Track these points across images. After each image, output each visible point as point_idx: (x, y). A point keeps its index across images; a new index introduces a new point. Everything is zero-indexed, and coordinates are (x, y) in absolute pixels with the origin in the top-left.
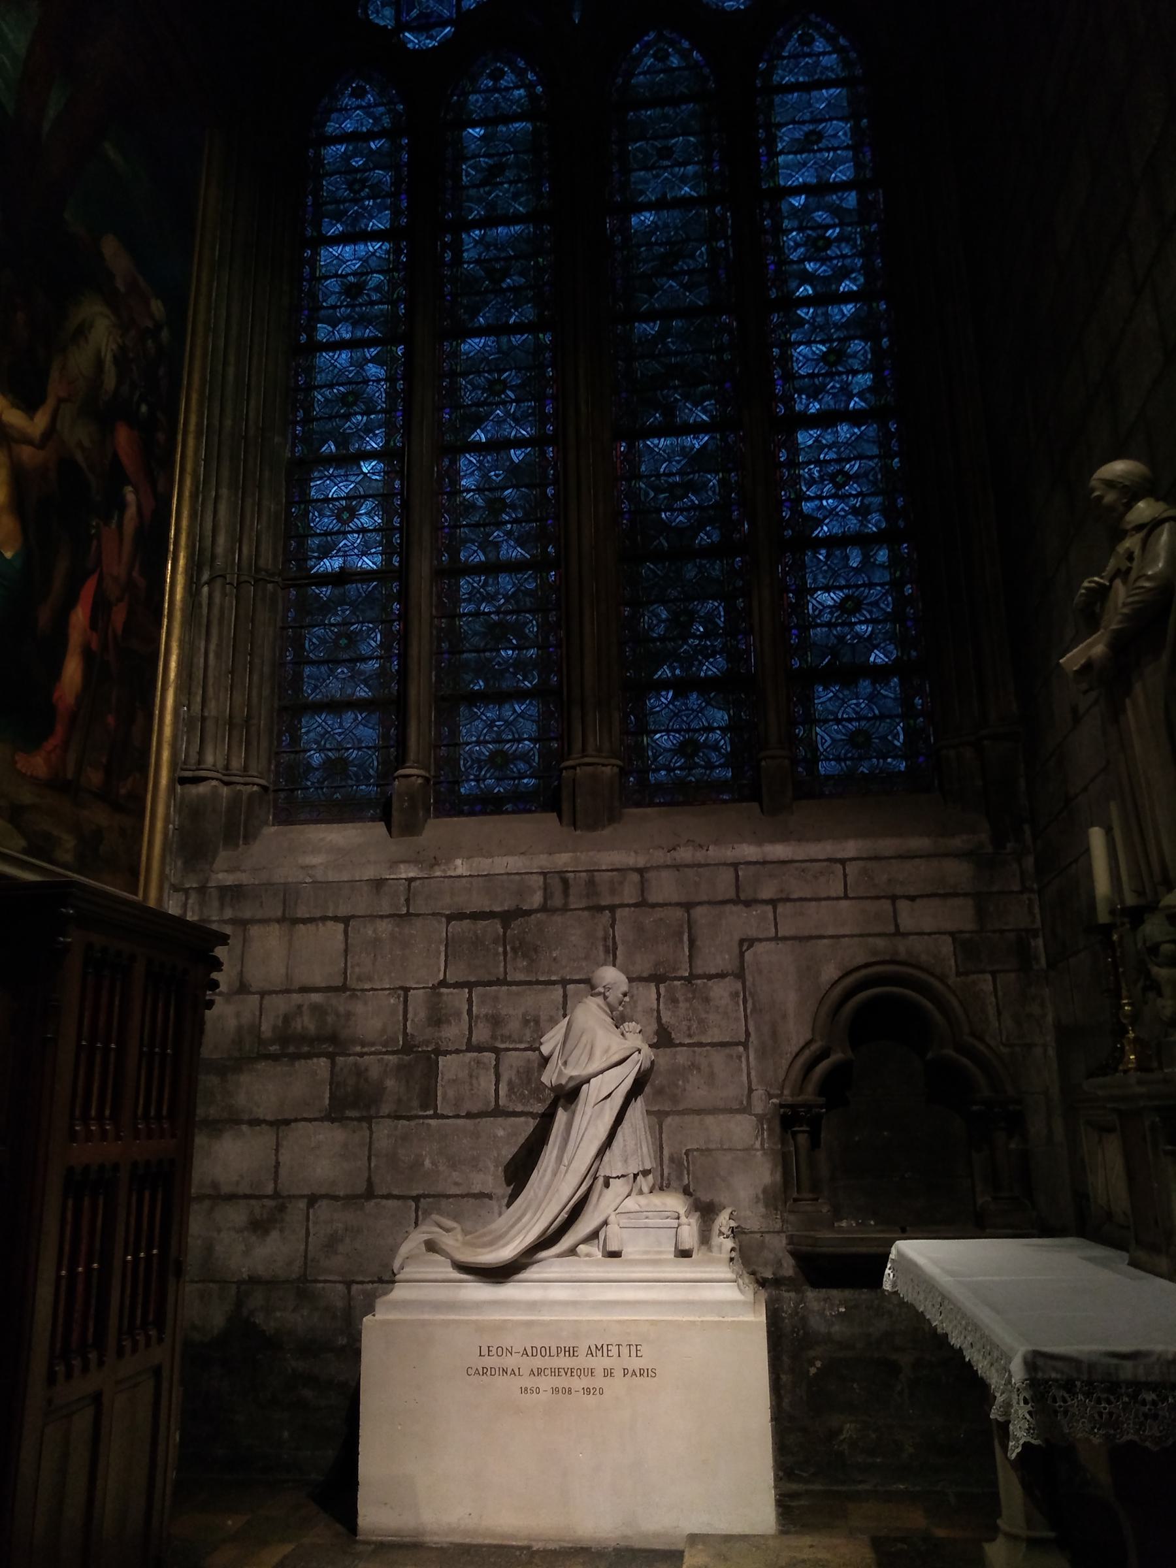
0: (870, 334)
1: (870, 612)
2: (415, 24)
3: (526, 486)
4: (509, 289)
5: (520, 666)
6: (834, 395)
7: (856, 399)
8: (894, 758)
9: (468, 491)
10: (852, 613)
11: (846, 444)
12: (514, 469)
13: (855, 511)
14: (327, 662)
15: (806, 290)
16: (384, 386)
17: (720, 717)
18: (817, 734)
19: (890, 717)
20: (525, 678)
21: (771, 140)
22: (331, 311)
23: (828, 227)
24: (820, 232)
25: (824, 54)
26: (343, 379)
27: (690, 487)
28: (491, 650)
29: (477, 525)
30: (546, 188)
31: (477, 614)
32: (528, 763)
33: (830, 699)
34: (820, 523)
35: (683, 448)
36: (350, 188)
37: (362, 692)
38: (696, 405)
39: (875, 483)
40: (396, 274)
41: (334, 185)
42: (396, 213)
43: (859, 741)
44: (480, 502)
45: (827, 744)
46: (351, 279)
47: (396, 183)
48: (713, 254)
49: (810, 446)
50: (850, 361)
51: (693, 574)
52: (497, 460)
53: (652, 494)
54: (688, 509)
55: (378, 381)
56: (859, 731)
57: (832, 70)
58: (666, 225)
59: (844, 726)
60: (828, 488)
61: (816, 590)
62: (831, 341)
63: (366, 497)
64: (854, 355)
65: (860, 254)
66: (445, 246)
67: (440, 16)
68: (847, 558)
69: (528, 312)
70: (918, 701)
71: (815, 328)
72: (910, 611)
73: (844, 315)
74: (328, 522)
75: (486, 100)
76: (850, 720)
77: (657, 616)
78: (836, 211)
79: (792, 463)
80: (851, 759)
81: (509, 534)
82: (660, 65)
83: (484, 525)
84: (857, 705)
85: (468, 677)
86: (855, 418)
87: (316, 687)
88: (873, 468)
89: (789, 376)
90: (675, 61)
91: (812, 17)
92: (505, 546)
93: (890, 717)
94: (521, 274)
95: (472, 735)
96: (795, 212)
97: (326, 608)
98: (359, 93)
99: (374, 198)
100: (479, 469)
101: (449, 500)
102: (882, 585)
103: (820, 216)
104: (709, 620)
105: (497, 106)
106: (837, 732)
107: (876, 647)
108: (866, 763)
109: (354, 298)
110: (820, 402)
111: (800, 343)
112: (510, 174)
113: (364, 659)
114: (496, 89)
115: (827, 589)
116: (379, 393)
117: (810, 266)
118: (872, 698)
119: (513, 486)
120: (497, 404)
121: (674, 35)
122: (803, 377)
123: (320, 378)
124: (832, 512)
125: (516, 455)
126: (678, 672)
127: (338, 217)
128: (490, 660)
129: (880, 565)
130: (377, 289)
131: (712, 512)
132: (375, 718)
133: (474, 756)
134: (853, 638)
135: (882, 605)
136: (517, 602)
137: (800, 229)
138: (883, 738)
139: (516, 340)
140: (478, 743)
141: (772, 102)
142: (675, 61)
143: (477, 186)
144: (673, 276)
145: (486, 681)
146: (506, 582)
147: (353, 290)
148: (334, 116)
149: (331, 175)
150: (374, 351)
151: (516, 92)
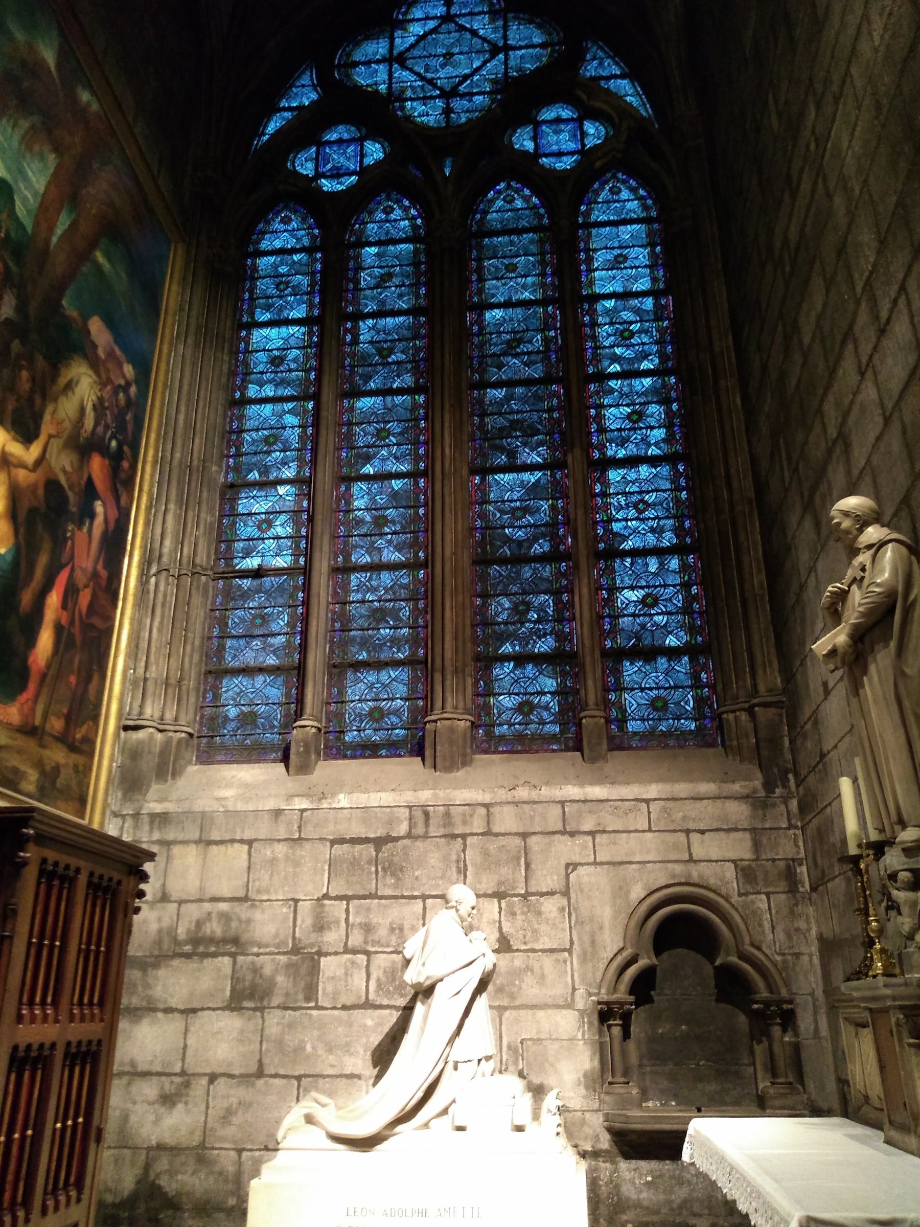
0: (665, 401)
1: (665, 606)
4: (394, 363)
5: (395, 641)
8: (686, 719)
10: (652, 606)
12: (394, 495)
13: (653, 530)
14: (245, 636)
15: (616, 368)
16: (298, 431)
17: (550, 684)
19: (682, 687)
21: (589, 260)
23: (631, 323)
24: (625, 326)
25: (628, 200)
26: (267, 425)
27: (526, 510)
28: (373, 629)
29: (366, 535)
30: (423, 291)
31: (363, 602)
34: (625, 538)
36: (277, 287)
37: (272, 661)
38: (532, 451)
39: (668, 510)
41: (265, 286)
42: (311, 306)
43: (658, 706)
44: (368, 519)
46: (276, 353)
47: (312, 285)
48: (546, 340)
51: (529, 575)
54: (525, 527)
55: (293, 427)
56: (658, 698)
58: (511, 320)
60: (632, 513)
61: (623, 588)
62: (634, 404)
63: (280, 512)
65: (656, 343)
66: (347, 331)
67: (348, 169)
68: (647, 565)
69: (408, 380)
70: (704, 675)
72: (696, 606)
75: (380, 228)
76: (651, 689)
77: (501, 605)
78: (637, 311)
79: (604, 494)
80: (652, 719)
81: (390, 542)
82: (508, 207)
83: (371, 535)
84: (657, 677)
85: (354, 650)
86: (653, 461)
87: (235, 656)
89: (602, 430)
90: (519, 203)
91: (620, 175)
93: (682, 687)
94: (403, 352)
96: (607, 312)
97: (246, 595)
98: (286, 221)
99: (295, 295)
100: (368, 494)
101: (344, 516)
102: (674, 586)
103: (626, 315)
104: (541, 609)
105: (387, 233)
107: (670, 633)
108: (664, 723)
109: (278, 366)
110: (625, 449)
111: (611, 406)
112: (397, 281)
113: (274, 635)
114: (387, 221)
115: (632, 588)
116: (293, 436)
117: (618, 351)
118: (667, 673)
119: (394, 507)
120: (383, 446)
121: (519, 185)
123: (249, 425)
124: (635, 531)
125: (396, 484)
126: (517, 648)
127: (268, 308)
130: (295, 360)
132: (280, 680)
133: (357, 711)
134: (652, 626)
136: (394, 593)
137: (611, 323)
138: (678, 704)
139: (398, 399)
140: (360, 701)
141: (590, 234)
142: (519, 203)
143: (372, 289)
144: (516, 356)
145: (369, 652)
146: (386, 578)
147: (276, 361)
148: (267, 236)
149: (264, 278)
150: (290, 405)
151: (402, 223)
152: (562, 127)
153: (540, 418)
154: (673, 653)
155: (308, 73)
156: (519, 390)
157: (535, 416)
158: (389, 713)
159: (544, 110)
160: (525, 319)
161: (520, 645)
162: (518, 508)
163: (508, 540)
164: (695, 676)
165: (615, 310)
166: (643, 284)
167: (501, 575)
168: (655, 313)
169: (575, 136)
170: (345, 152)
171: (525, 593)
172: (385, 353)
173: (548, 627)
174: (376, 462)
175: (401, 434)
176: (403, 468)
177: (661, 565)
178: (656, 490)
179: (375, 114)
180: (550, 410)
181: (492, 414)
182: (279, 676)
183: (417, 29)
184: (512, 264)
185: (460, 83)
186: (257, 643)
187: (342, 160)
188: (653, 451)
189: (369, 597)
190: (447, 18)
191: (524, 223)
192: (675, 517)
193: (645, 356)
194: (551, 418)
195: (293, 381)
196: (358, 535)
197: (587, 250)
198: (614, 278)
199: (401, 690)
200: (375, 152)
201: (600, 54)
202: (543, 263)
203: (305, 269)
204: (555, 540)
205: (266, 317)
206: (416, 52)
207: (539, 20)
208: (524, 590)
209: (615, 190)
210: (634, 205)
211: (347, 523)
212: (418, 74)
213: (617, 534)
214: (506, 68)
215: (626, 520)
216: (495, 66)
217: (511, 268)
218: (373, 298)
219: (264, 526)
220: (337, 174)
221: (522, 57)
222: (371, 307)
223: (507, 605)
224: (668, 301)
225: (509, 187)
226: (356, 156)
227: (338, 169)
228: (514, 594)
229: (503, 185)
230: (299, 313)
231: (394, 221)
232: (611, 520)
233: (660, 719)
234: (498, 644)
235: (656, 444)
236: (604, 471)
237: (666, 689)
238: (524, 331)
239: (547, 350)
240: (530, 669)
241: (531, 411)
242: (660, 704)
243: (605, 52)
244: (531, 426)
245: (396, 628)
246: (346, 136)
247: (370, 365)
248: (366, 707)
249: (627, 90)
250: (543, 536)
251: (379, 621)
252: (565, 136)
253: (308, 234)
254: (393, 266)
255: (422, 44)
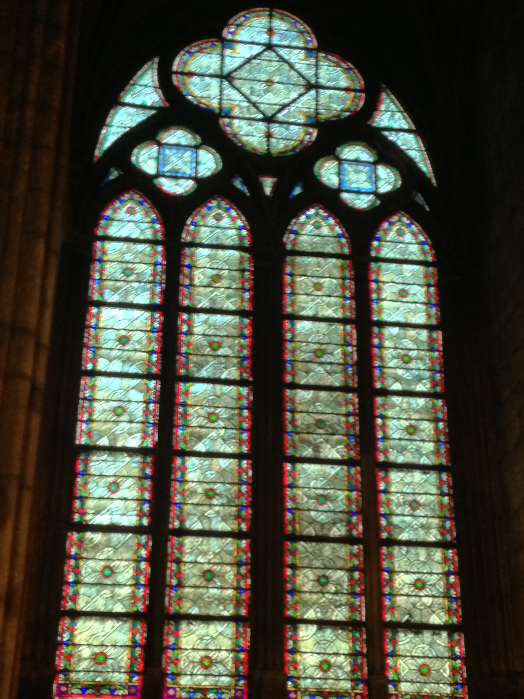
0: (436, 420)
2: (168, 174)
3: (229, 483)
5: (221, 601)
6: (412, 453)
7: (424, 457)
8: (444, 684)
9: (193, 482)
10: (420, 589)
11: (419, 484)
12: (222, 472)
15: (397, 386)
17: (344, 647)
18: (400, 664)
19: (441, 658)
20: (225, 609)
21: (379, 290)
22: (109, 351)
24: (406, 351)
25: (410, 243)
28: (203, 587)
29: (197, 505)
30: (247, 295)
32: (224, 666)
33: (407, 643)
35: (325, 472)
37: (119, 608)
39: (433, 510)
40: (151, 334)
42: (153, 294)
43: (424, 671)
45: (406, 672)
46: (123, 333)
47: (154, 275)
48: (345, 354)
49: (398, 482)
50: (422, 433)
52: (211, 464)
53: (306, 499)
54: (326, 512)
55: (138, 402)
56: (424, 665)
57: (415, 254)
58: (318, 332)
59: (416, 661)
63: (128, 477)
64: (423, 431)
65: (429, 370)
68: (417, 554)
69: (233, 373)
71: (402, 410)
73: (418, 405)
74: (102, 491)
75: (211, 232)
76: (418, 657)
77: (307, 577)
80: (419, 682)
82: (316, 232)
83: (202, 505)
84: (423, 648)
86: (424, 469)
88: (433, 501)
89: (385, 438)
90: (325, 230)
92: (214, 521)
93: (441, 658)
94: (229, 347)
95: (189, 645)
96: (392, 337)
97: (96, 547)
98: (131, 212)
101: (180, 486)
104: (338, 583)
105: (217, 238)
106: (412, 664)
107: (434, 612)
108: (428, 686)
109: (124, 344)
110: (404, 455)
111: (393, 418)
112: (225, 283)
113: (119, 585)
114: (218, 227)
115: (407, 572)
116: (137, 410)
117: (400, 372)
118: (431, 645)
121: (326, 214)
122: (394, 439)
124: (409, 525)
125: (224, 463)
127: (115, 290)
128: (202, 594)
129: (437, 562)
130: (139, 342)
131: (340, 515)
132: (127, 626)
133: (191, 659)
134: (421, 605)
135: (438, 587)
136: (221, 558)
137: (395, 348)
138: (437, 671)
139: (226, 389)
140: (194, 649)
142: (325, 230)
143: (205, 287)
144: (321, 364)
145: (200, 608)
146: (215, 544)
147: (123, 340)
148: (115, 223)
149: (112, 261)
152: (361, 168)
153: (339, 420)
154: (436, 629)
155: (150, 72)
156: (323, 394)
157: (335, 418)
158: (217, 663)
159: (347, 150)
160: (328, 334)
161: (322, 612)
162: (321, 495)
163: (313, 522)
164: (451, 649)
165: (398, 337)
166: (420, 319)
167: (307, 551)
168: (429, 345)
169: (370, 177)
170: (181, 157)
171: (326, 568)
172: (215, 346)
173: (344, 599)
174: (206, 441)
175: (228, 419)
176: (229, 449)
177: (429, 555)
178: (426, 494)
179: (208, 126)
180: (348, 415)
181: (302, 412)
182: (125, 621)
183: (244, 52)
184: (318, 283)
185: (279, 111)
186: (107, 592)
187: (180, 163)
188: (424, 461)
189: (200, 559)
190: (269, 47)
191: (328, 249)
192: (439, 517)
193: (419, 379)
194: (347, 422)
195: (139, 361)
196: (192, 504)
197: (377, 281)
198: (398, 309)
199: (227, 643)
200: (209, 163)
201: (392, 107)
202: (344, 287)
203: (148, 259)
204: (350, 525)
205: (115, 298)
206: (242, 73)
207: (344, 65)
208: (324, 564)
209: (401, 232)
210: (414, 248)
211: (182, 493)
212: (243, 95)
213: (396, 527)
214: (317, 105)
215: (403, 515)
216: (307, 101)
217: (318, 287)
218: (206, 296)
219: (113, 488)
220: (175, 176)
221: (330, 97)
222: (204, 304)
223: (312, 577)
224: (438, 335)
225: (317, 214)
226: (191, 162)
227: (177, 171)
228: (316, 568)
229: (311, 212)
230: (144, 299)
231: (220, 227)
232: (391, 514)
233: (425, 683)
234: (304, 609)
235: (427, 455)
236: (387, 471)
237: (430, 658)
238: (327, 344)
239: (345, 365)
240: (328, 633)
241: (332, 413)
242: (425, 670)
243: (397, 107)
244: (331, 427)
245: (222, 588)
246: (184, 142)
247: (203, 355)
248: (197, 656)
249: (411, 145)
250: (341, 521)
251: (209, 580)
252: (363, 177)
253: (152, 228)
254: (221, 269)
255: (248, 66)
